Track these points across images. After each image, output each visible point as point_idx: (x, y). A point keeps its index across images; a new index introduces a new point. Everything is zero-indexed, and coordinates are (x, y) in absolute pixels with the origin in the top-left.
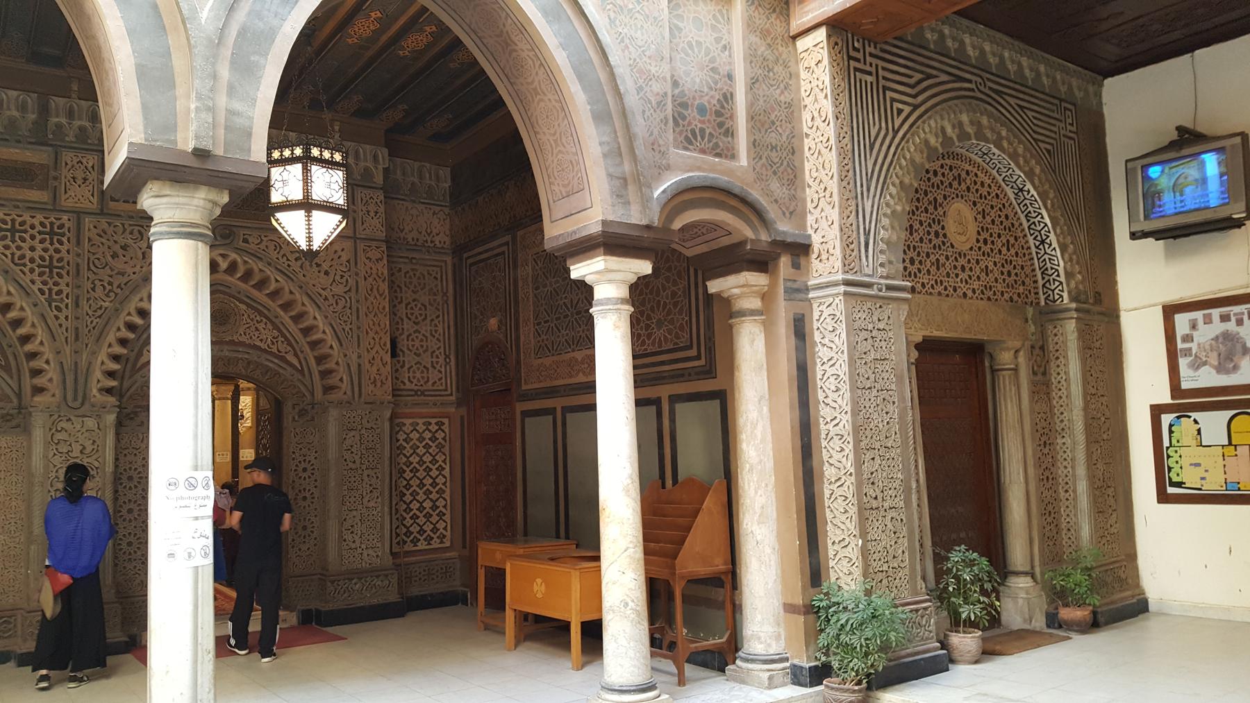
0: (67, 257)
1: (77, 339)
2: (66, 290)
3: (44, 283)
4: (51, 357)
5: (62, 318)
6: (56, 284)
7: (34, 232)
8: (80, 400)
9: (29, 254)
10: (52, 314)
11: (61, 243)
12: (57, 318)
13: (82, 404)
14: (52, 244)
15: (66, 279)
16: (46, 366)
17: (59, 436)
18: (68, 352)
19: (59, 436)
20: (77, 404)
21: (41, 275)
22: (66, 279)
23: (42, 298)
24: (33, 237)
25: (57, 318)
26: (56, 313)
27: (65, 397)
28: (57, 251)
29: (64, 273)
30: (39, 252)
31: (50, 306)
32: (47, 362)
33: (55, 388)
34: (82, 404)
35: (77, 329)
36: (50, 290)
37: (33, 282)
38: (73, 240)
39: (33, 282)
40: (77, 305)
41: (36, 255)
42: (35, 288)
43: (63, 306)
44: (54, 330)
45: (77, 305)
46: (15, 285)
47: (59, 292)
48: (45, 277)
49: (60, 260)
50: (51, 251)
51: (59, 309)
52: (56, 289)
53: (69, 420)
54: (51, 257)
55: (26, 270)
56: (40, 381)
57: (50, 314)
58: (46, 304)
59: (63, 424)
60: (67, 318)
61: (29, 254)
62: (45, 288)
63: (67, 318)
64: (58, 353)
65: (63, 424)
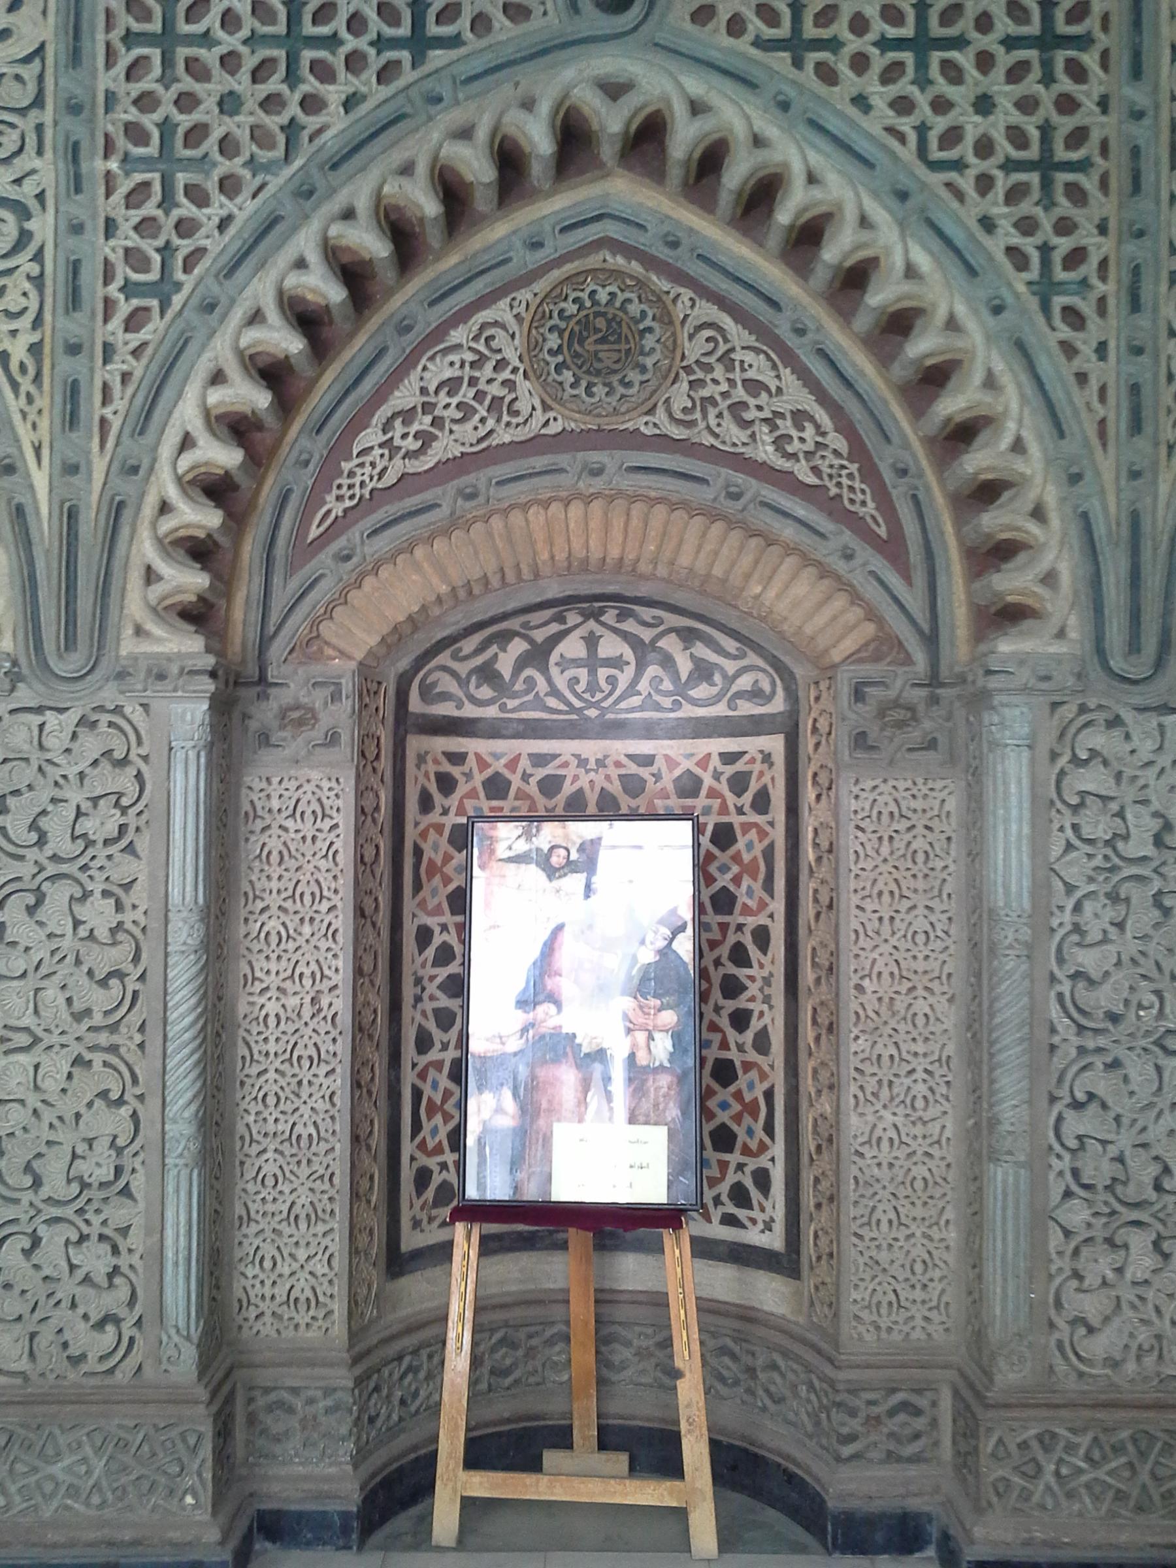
0: (1101, 126)
1: (1136, 426)
2: (1099, 247)
3: (1027, 226)
4: (1051, 497)
5: (1087, 350)
6: (1064, 227)
7: (989, 42)
8: (1150, 644)
9: (974, 126)
10: (1052, 339)
11: (1077, 72)
12: (1069, 349)
13: (1159, 664)
14: (1048, 79)
15: (1101, 206)
16: (1033, 528)
17: (1092, 780)
18: (1108, 476)
19: (1092, 780)
20: (1137, 668)
21: (1014, 195)
22: (1101, 206)
23: (1020, 282)
24: (985, 61)
25: (1069, 349)
26: (1065, 332)
27: (1100, 651)
28: (1067, 104)
29: (1089, 183)
30: (1006, 114)
31: (1046, 307)
32: (1038, 513)
33: (1063, 607)
34: (1159, 664)
35: (1135, 389)
36: (1045, 249)
37: (987, 223)
38: (1121, 61)
39: (987, 223)
40: (1135, 305)
41: (996, 126)
42: (996, 245)
43: (1087, 308)
44: (1057, 394)
45: (1135, 305)
46: (936, 244)
47: (1076, 257)
48: (1027, 207)
49: (1078, 137)
50: (1047, 109)
51: (1073, 317)
52: (1064, 244)
53: (1115, 722)
54: (1046, 130)
55: (966, 183)
56: (1013, 582)
57: (1048, 338)
58: (1033, 303)
59: (1096, 739)
60: (1101, 350)
61: (974, 126)
62: (1029, 245)
63: (1101, 350)
64: (1075, 479)
65: (1096, 739)
